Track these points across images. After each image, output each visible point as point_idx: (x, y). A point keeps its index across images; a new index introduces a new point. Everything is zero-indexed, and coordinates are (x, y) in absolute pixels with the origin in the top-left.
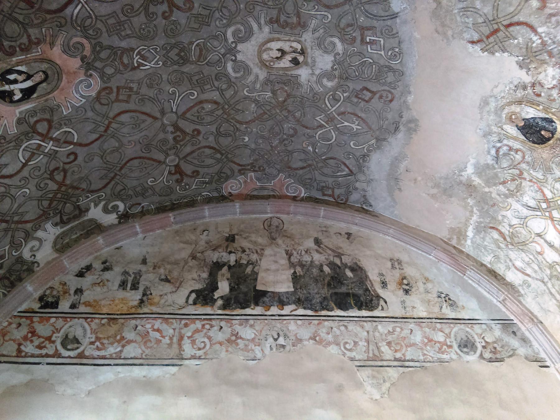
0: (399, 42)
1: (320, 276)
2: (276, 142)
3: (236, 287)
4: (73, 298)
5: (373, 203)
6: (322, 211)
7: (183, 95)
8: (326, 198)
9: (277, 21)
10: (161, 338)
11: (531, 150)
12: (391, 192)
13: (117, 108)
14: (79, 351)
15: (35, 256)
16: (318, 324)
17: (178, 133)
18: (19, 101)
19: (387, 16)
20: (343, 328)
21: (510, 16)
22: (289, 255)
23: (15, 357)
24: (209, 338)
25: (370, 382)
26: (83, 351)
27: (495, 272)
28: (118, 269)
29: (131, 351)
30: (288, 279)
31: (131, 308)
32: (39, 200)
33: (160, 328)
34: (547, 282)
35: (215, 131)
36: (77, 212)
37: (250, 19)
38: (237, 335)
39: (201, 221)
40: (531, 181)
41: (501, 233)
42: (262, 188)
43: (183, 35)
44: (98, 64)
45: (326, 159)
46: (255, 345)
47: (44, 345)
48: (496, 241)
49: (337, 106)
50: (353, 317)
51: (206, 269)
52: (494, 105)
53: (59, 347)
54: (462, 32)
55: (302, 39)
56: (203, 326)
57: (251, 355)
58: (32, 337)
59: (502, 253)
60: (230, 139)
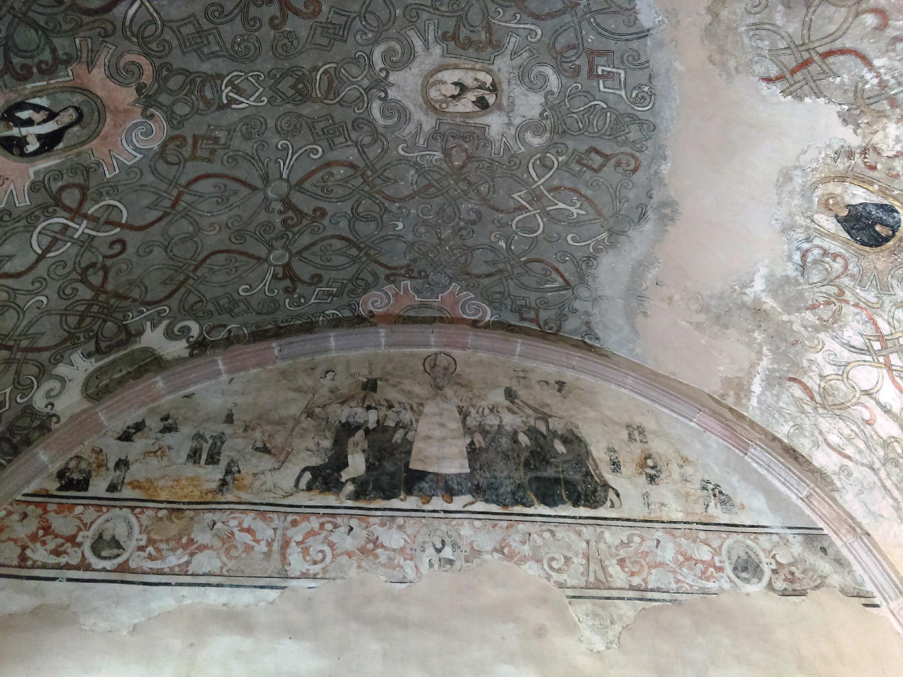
0: (650, 76)
1: (513, 450)
2: (447, 233)
3: (377, 463)
4: (111, 475)
5: (601, 335)
6: (519, 344)
7: (300, 152)
8: (526, 324)
10: (253, 544)
11: (859, 255)
12: (630, 316)
13: (192, 169)
14: (120, 560)
15: (53, 405)
16: (507, 527)
17: (290, 214)
18: (35, 153)
20: (547, 535)
21: (832, 38)
22: (464, 414)
23: (15, 567)
24: (332, 545)
25: (590, 623)
26: (126, 562)
27: (794, 451)
28: (186, 430)
29: (205, 562)
30: (461, 453)
31: (206, 494)
32: (62, 315)
33: (253, 527)
34: (879, 469)
35: (349, 212)
36: (123, 336)
37: (412, 33)
38: (375, 542)
39: (324, 356)
40: (856, 305)
41: (806, 388)
42: (423, 306)
43: (303, 55)
44: (164, 99)
45: (525, 263)
46: (405, 559)
48: (797, 401)
49: (548, 176)
50: (565, 517)
51: (328, 434)
52: (800, 181)
53: (89, 554)
55: (495, 68)
56: (322, 525)
57: (398, 574)
58: (44, 535)
59: (806, 419)
60: (373, 226)
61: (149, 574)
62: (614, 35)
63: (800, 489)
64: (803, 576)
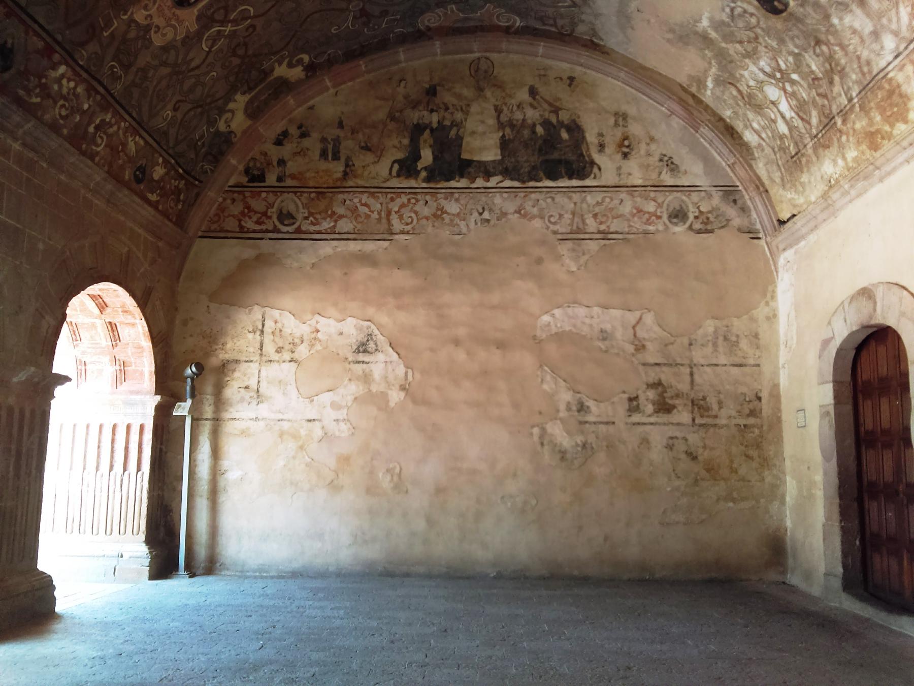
1: (531, 139)
3: (440, 155)
5: (604, 37)
10: (369, 213)
14: (296, 226)
15: (229, 126)
16: (524, 196)
20: (549, 200)
22: (498, 111)
23: (238, 232)
24: (416, 213)
27: (732, 128)
28: (315, 135)
29: (345, 225)
31: (337, 181)
33: (368, 202)
38: (442, 210)
40: (766, 47)
41: (739, 91)
46: (460, 220)
47: (261, 220)
48: (734, 97)
50: (562, 187)
53: (277, 223)
56: (409, 200)
57: (456, 229)
59: (740, 110)
61: (313, 233)
63: (729, 158)
64: (715, 220)
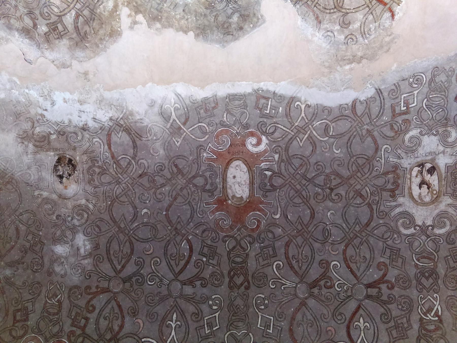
0: (403, 80)
9: (393, 191)
19: (380, 97)
37: (393, 214)
54: (385, 29)
55: (408, 167)
62: (382, 107)
